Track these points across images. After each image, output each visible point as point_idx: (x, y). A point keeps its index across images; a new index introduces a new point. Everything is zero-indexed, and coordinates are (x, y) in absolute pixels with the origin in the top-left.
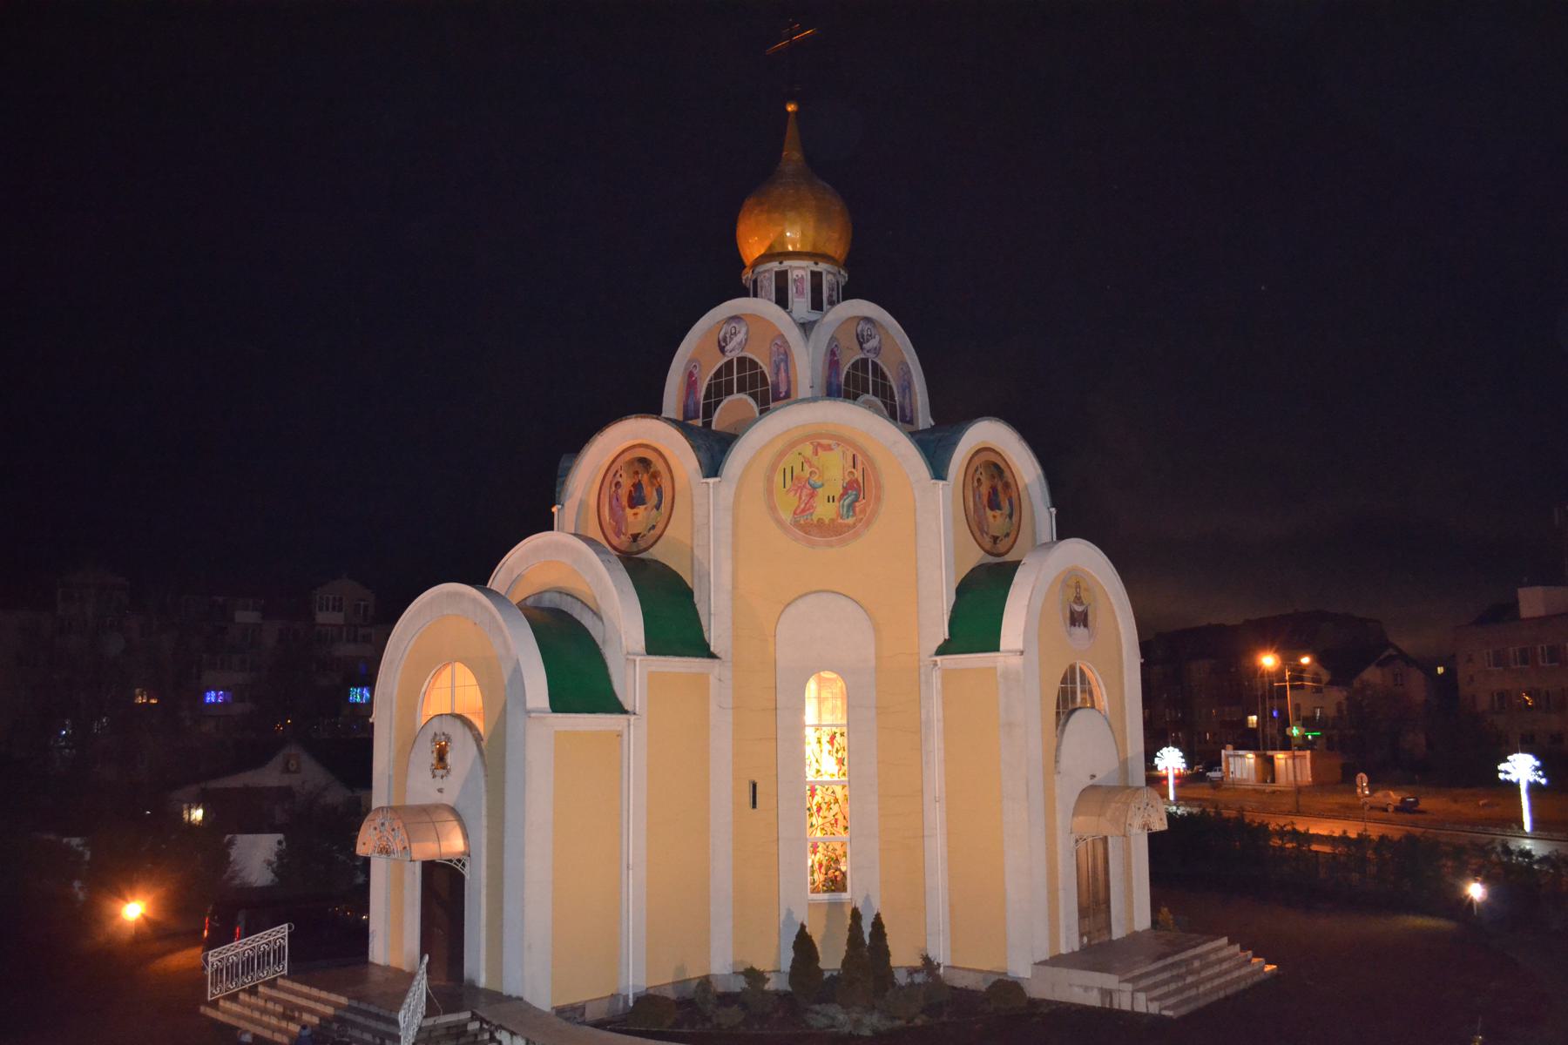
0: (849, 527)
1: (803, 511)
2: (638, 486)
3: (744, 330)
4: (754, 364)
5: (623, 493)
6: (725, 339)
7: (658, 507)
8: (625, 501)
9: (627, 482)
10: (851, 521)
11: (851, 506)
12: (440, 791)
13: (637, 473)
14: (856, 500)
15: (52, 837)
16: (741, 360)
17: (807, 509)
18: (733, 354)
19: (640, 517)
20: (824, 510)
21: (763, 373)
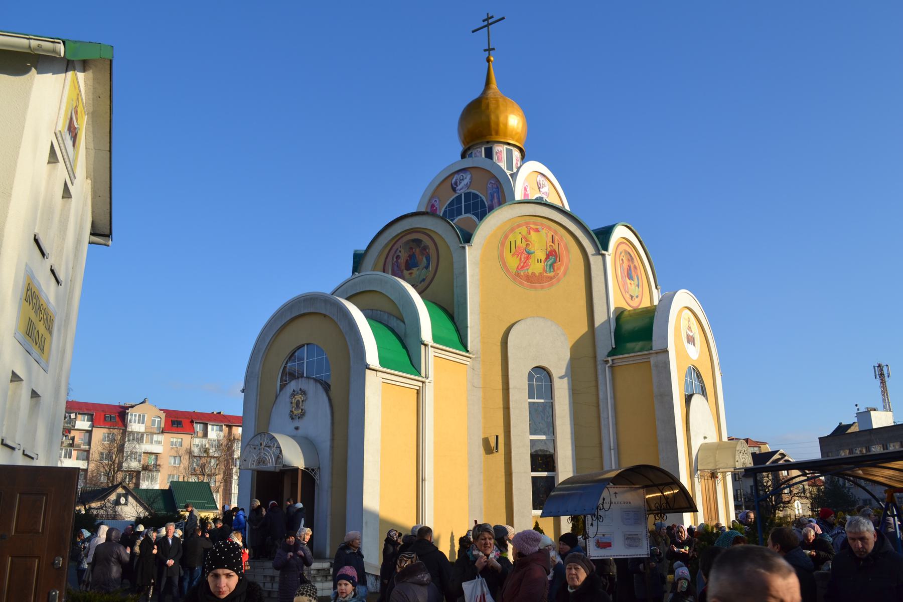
0: (551, 278)
1: (523, 267)
2: (412, 256)
3: (469, 177)
4: (476, 196)
5: (402, 261)
6: (456, 183)
7: (427, 267)
8: (403, 267)
9: (404, 255)
10: (552, 274)
11: (552, 266)
12: (297, 428)
13: (411, 248)
14: (555, 262)
15: (763, 571)
16: (467, 195)
17: (524, 265)
18: (462, 189)
19: (414, 275)
20: (536, 267)
21: (482, 201)
